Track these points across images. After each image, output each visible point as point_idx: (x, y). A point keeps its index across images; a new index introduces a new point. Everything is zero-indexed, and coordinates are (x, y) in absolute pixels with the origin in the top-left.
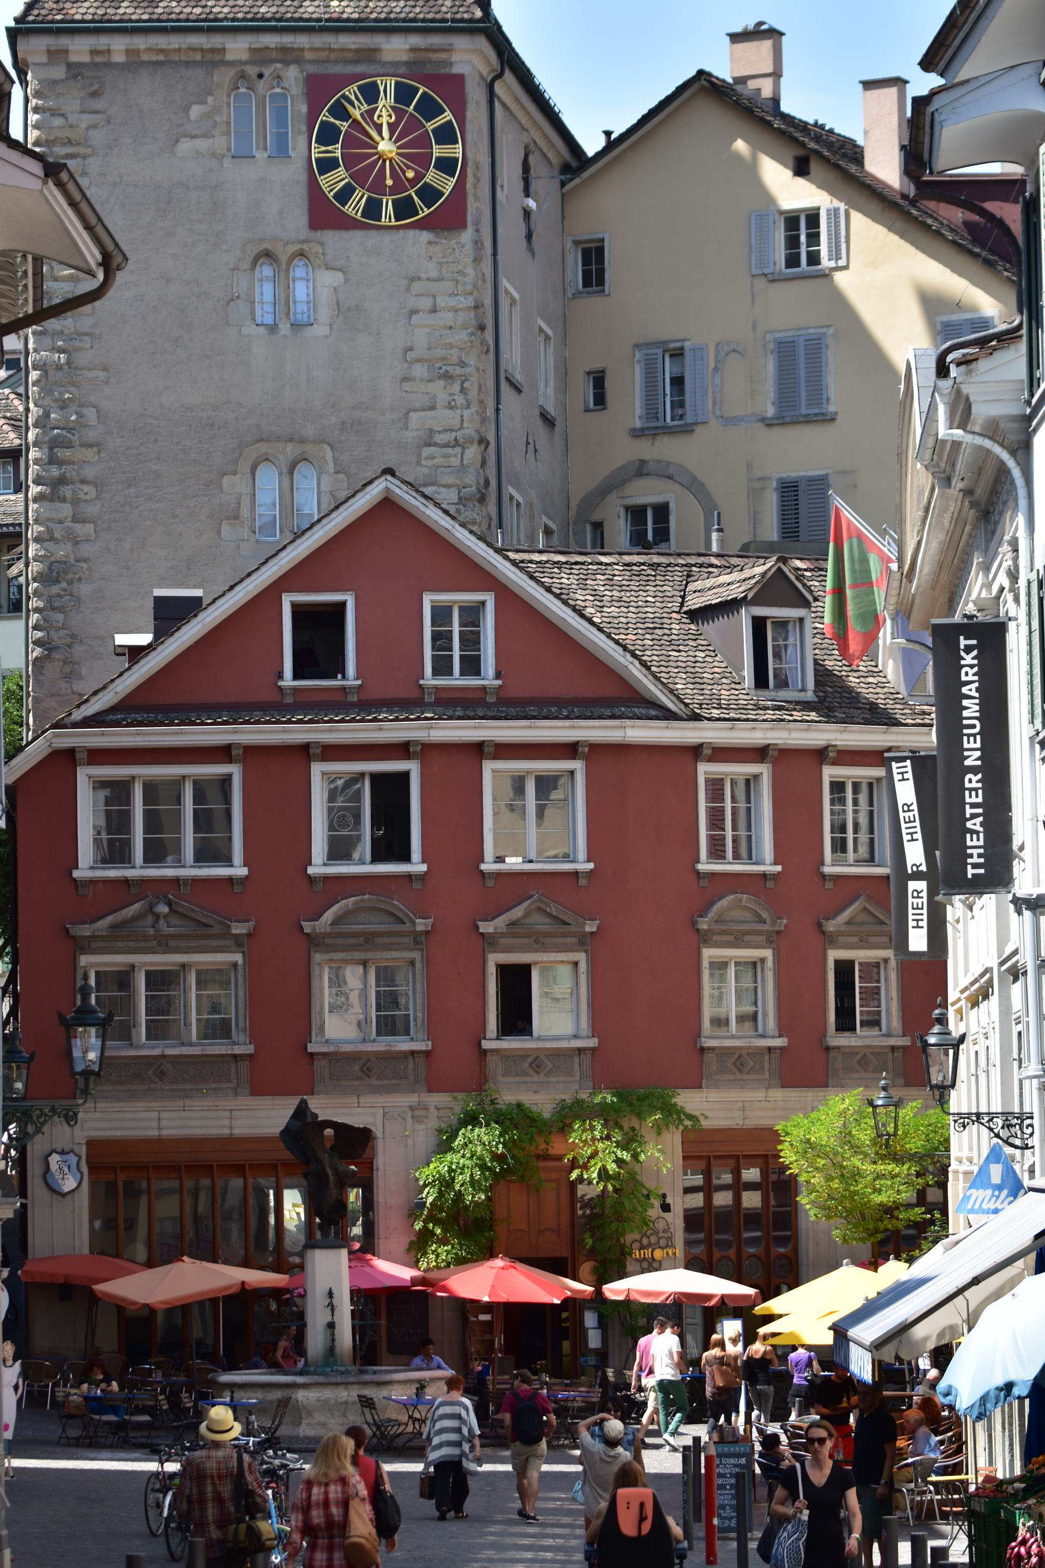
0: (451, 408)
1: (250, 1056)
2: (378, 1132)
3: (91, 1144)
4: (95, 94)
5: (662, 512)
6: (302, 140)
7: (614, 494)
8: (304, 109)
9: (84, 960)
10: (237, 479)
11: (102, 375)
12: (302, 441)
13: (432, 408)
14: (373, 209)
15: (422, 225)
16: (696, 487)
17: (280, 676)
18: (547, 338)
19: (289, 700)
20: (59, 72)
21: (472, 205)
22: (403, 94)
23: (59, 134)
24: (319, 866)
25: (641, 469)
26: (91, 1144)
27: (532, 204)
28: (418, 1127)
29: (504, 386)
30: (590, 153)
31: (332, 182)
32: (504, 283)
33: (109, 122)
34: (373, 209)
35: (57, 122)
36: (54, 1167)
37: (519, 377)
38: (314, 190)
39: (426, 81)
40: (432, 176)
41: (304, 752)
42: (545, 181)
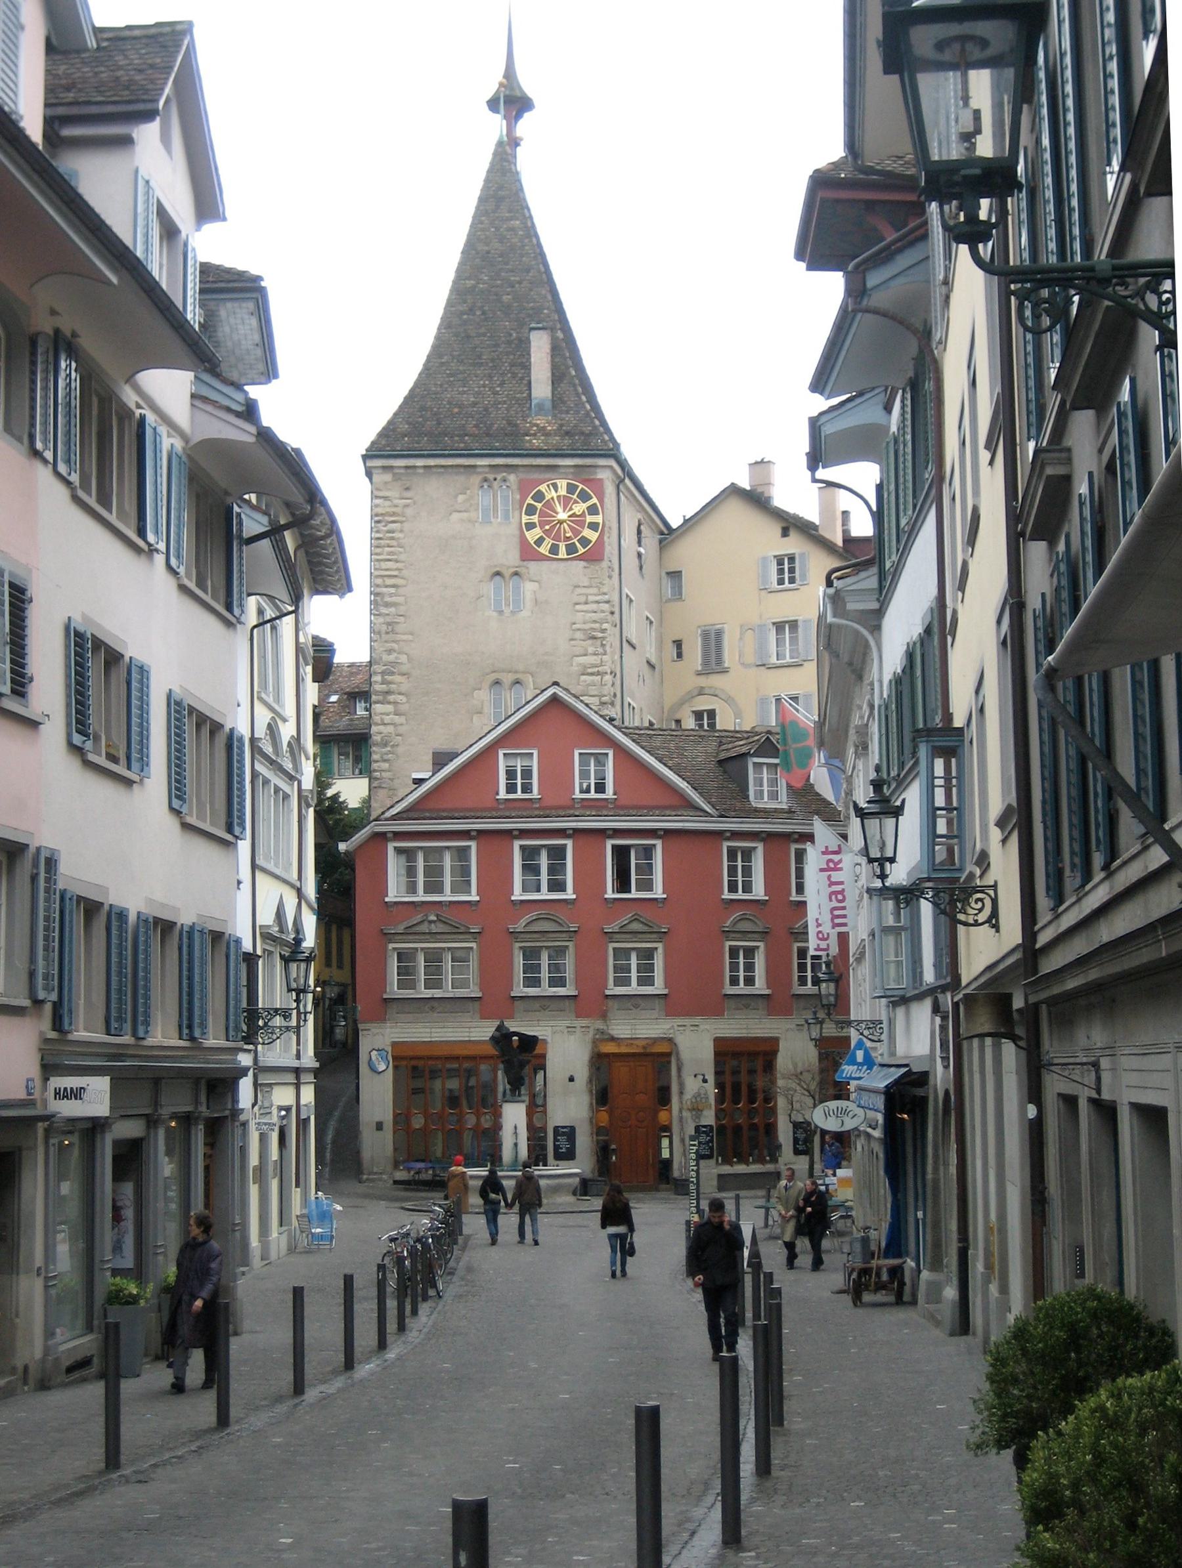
0: (595, 654)
2: (549, 1040)
4: (407, 489)
5: (712, 714)
6: (517, 513)
7: (687, 705)
8: (518, 497)
9: (391, 946)
10: (481, 692)
11: (410, 637)
12: (516, 672)
13: (586, 655)
14: (554, 549)
15: (581, 558)
16: (729, 700)
17: (497, 794)
18: (651, 622)
19: (501, 807)
20: (388, 477)
21: (608, 549)
22: (571, 489)
23: (388, 510)
24: (518, 894)
25: (701, 692)
27: (642, 550)
29: (625, 644)
30: (674, 526)
31: (532, 536)
32: (626, 590)
33: (415, 503)
34: (554, 549)
35: (387, 503)
36: (374, 1058)
37: (634, 641)
38: (523, 541)
39: (583, 482)
40: (587, 533)
41: (509, 834)
42: (651, 540)
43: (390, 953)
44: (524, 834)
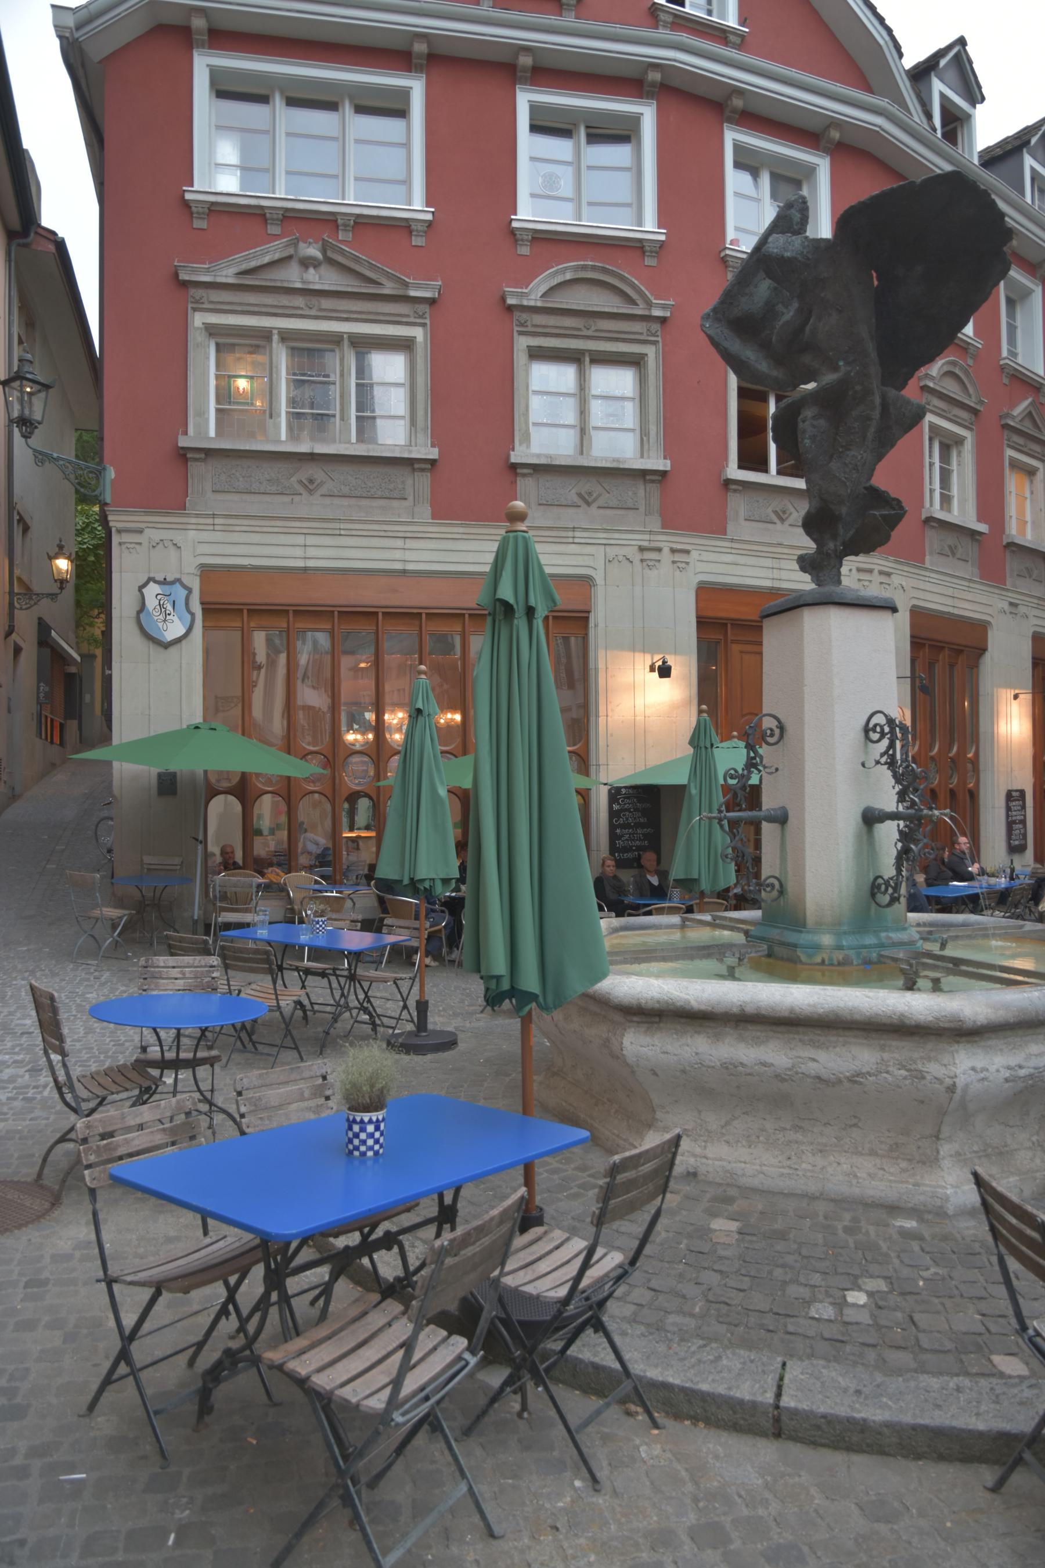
1: (433, 462)
2: (599, 579)
3: (207, 572)
9: (199, 320)
26: (207, 572)
28: (653, 573)
43: (196, 336)
44: (550, 72)
